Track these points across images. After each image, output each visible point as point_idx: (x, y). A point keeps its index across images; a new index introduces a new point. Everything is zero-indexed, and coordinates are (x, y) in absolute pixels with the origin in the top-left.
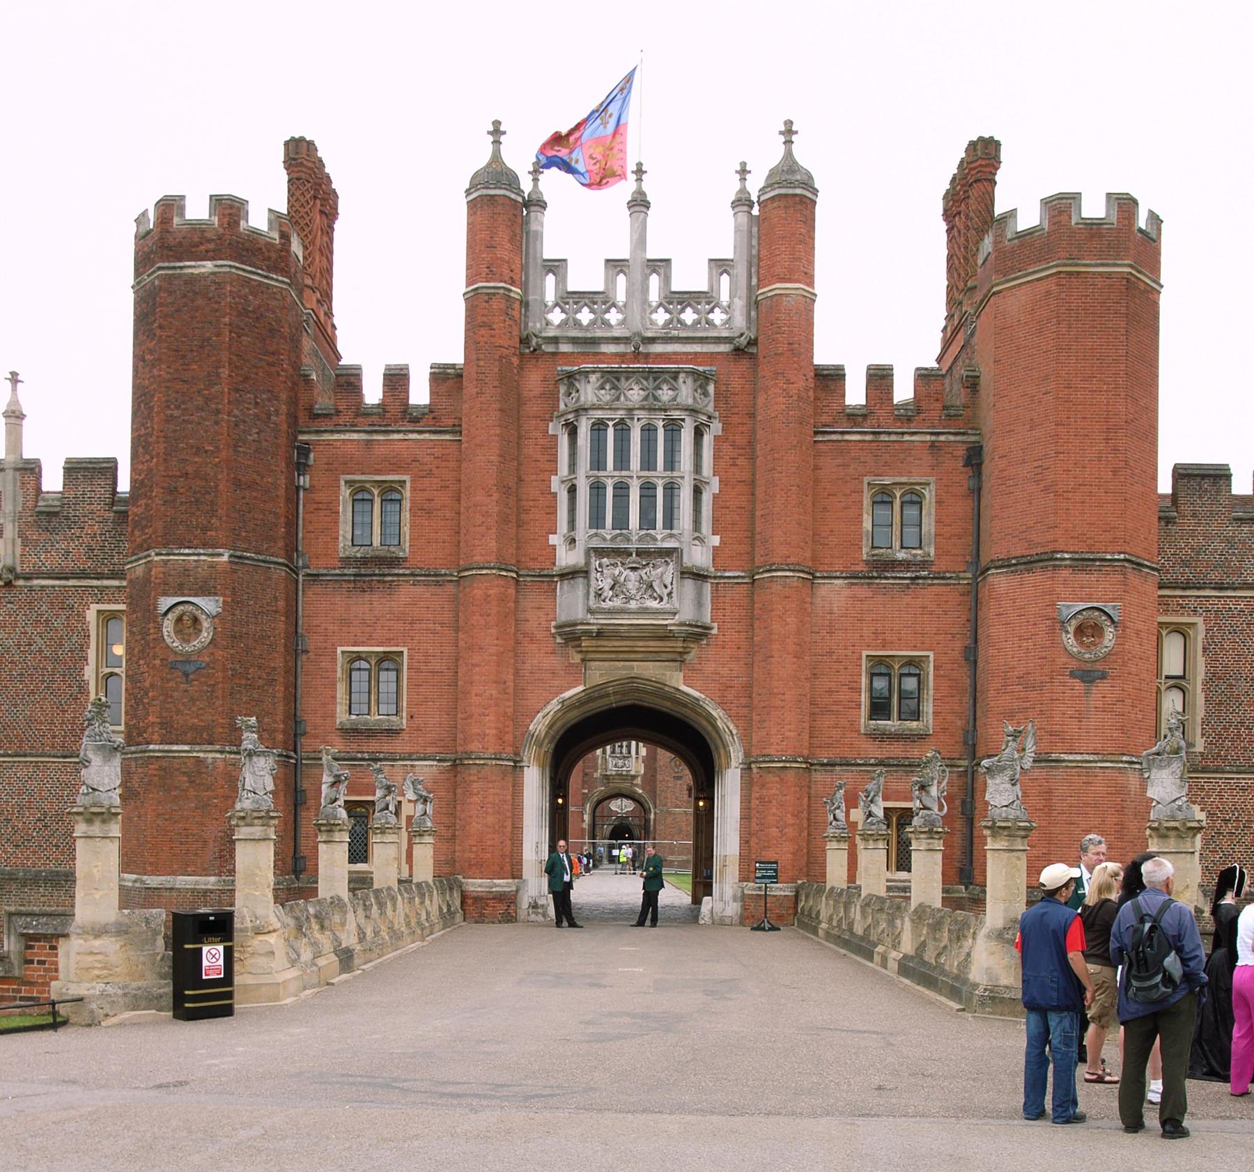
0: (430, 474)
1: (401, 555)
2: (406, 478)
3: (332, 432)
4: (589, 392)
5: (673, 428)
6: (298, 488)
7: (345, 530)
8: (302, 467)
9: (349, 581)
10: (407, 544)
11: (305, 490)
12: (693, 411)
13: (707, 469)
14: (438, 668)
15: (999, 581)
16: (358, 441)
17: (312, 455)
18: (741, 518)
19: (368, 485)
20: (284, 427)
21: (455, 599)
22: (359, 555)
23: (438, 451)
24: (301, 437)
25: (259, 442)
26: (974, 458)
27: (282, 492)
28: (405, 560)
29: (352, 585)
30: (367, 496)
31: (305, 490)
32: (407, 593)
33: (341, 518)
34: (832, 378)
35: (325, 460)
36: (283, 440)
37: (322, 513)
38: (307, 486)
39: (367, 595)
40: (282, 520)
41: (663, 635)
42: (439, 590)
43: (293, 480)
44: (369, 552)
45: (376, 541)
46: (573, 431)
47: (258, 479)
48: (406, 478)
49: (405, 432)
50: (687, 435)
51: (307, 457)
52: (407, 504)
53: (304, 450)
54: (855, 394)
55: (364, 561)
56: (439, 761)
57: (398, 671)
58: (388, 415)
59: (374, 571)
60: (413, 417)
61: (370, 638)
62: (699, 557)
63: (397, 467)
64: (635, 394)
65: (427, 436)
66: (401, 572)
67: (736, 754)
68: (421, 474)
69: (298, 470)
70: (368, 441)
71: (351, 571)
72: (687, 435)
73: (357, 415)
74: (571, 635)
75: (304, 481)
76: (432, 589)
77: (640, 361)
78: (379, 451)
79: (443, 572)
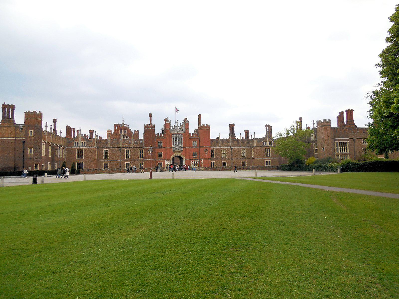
4: (174, 136)
5: (180, 138)
12: (181, 137)
13: (182, 140)
15: (201, 148)
18: (184, 143)
21: (166, 150)
26: (199, 139)
32: (162, 149)
34: (190, 134)
41: (180, 151)
46: (173, 138)
50: (181, 138)
54: (192, 135)
59: (160, 147)
60: (162, 137)
62: (182, 146)
64: (177, 136)
67: (184, 159)
72: (181, 138)
74: (174, 151)
77: (178, 134)
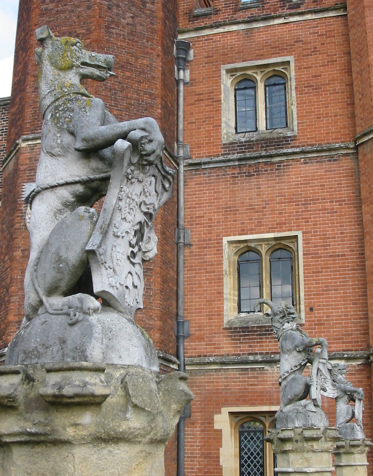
0: (315, 50)
1: (289, 134)
2: (290, 58)
3: (211, 27)
6: (178, 82)
7: (228, 118)
8: (183, 62)
9: (234, 167)
10: (295, 123)
11: (185, 84)
14: (339, 250)
16: (237, 32)
17: (191, 52)
19: (250, 72)
20: (160, 14)
22: (243, 140)
23: (321, 30)
24: (180, 37)
25: (133, 25)
27: (158, 74)
28: (294, 138)
29: (237, 171)
30: (251, 84)
31: (185, 84)
33: (224, 105)
35: (205, 54)
36: (158, 26)
37: (202, 104)
38: (188, 79)
39: (254, 180)
40: (159, 101)
42: (334, 166)
43: (172, 72)
44: (254, 136)
45: (262, 125)
47: (132, 60)
48: (290, 58)
49: (285, 17)
51: (187, 52)
52: (292, 84)
53: (185, 47)
55: (250, 145)
56: (348, 359)
57: (292, 258)
58: (267, 6)
61: (260, 224)
63: (280, 48)
65: (309, 17)
66: (290, 151)
68: (305, 53)
69: (178, 65)
70: (248, 30)
71: (236, 156)
73: (236, 11)
75: (185, 75)
76: (326, 165)
78: (261, 38)
79: (337, 145)
